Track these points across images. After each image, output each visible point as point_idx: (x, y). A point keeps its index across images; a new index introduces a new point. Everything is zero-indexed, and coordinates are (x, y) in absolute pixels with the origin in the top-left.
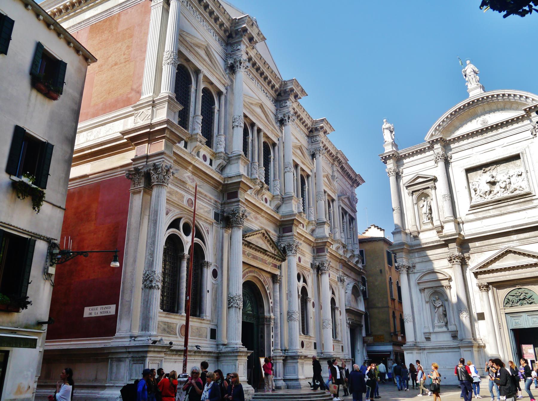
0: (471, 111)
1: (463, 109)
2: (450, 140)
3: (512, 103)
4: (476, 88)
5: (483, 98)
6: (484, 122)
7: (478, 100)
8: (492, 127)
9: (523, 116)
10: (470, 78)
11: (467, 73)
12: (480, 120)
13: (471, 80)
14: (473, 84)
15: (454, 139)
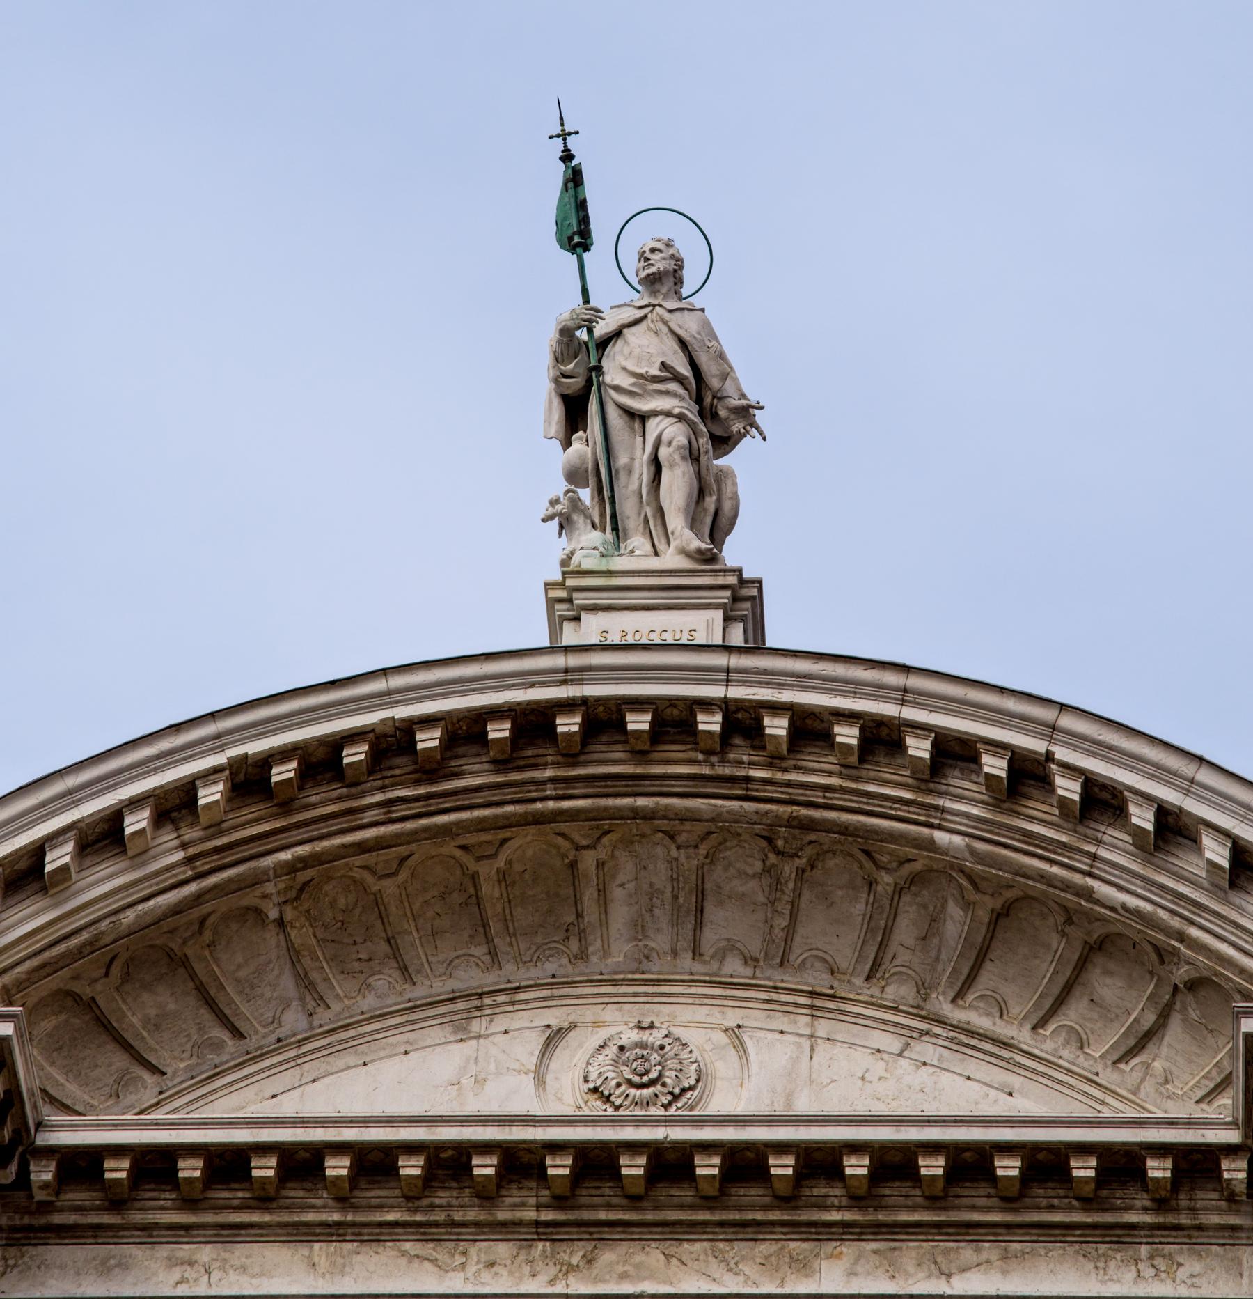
0: (524, 843)
1: (431, 769)
2: (82, 1165)
3: (1099, 943)
4: (670, 593)
5: (743, 722)
6: (646, 1073)
7: (674, 721)
8: (744, 1163)
9: (1196, 1164)
10: (633, 457)
11: (614, 374)
12: (603, 1030)
13: (636, 479)
14: (638, 542)
15: (155, 1165)
